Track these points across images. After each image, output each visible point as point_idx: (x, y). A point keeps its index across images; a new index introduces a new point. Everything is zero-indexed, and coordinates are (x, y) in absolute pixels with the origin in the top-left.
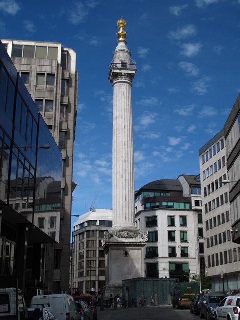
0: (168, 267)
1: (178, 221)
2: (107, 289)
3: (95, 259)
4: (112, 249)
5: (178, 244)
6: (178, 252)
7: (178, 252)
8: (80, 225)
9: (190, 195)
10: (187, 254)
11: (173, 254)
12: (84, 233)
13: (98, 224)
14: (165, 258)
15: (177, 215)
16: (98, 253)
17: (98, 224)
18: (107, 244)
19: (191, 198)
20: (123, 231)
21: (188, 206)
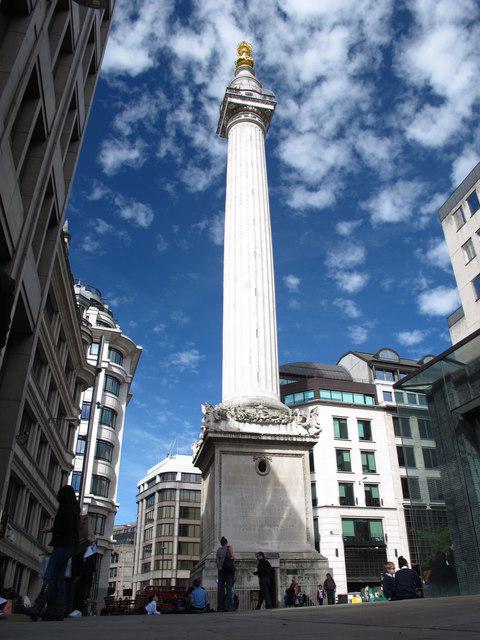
0: (338, 527)
1: (354, 430)
2: (207, 565)
3: (172, 503)
4: (223, 452)
5: (357, 477)
6: (359, 494)
7: (359, 494)
8: (148, 482)
9: (371, 380)
10: (378, 499)
11: (347, 500)
12: (154, 494)
13: (179, 477)
14: (332, 506)
15: (352, 416)
16: (176, 528)
17: (179, 477)
18: (210, 435)
19: (375, 386)
20: (253, 406)
21: (370, 401)
